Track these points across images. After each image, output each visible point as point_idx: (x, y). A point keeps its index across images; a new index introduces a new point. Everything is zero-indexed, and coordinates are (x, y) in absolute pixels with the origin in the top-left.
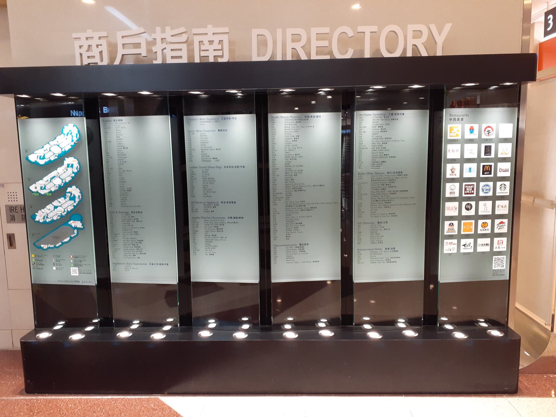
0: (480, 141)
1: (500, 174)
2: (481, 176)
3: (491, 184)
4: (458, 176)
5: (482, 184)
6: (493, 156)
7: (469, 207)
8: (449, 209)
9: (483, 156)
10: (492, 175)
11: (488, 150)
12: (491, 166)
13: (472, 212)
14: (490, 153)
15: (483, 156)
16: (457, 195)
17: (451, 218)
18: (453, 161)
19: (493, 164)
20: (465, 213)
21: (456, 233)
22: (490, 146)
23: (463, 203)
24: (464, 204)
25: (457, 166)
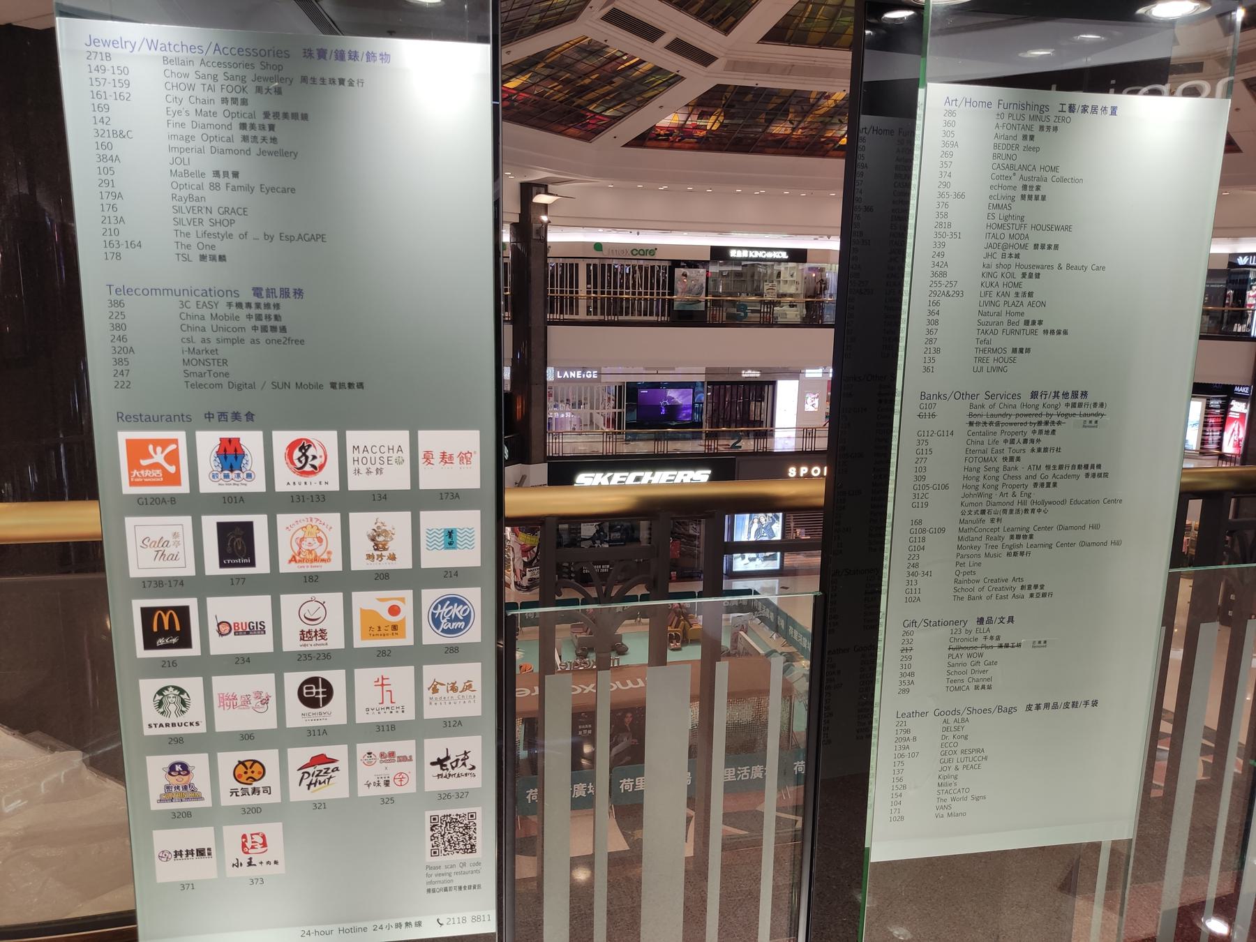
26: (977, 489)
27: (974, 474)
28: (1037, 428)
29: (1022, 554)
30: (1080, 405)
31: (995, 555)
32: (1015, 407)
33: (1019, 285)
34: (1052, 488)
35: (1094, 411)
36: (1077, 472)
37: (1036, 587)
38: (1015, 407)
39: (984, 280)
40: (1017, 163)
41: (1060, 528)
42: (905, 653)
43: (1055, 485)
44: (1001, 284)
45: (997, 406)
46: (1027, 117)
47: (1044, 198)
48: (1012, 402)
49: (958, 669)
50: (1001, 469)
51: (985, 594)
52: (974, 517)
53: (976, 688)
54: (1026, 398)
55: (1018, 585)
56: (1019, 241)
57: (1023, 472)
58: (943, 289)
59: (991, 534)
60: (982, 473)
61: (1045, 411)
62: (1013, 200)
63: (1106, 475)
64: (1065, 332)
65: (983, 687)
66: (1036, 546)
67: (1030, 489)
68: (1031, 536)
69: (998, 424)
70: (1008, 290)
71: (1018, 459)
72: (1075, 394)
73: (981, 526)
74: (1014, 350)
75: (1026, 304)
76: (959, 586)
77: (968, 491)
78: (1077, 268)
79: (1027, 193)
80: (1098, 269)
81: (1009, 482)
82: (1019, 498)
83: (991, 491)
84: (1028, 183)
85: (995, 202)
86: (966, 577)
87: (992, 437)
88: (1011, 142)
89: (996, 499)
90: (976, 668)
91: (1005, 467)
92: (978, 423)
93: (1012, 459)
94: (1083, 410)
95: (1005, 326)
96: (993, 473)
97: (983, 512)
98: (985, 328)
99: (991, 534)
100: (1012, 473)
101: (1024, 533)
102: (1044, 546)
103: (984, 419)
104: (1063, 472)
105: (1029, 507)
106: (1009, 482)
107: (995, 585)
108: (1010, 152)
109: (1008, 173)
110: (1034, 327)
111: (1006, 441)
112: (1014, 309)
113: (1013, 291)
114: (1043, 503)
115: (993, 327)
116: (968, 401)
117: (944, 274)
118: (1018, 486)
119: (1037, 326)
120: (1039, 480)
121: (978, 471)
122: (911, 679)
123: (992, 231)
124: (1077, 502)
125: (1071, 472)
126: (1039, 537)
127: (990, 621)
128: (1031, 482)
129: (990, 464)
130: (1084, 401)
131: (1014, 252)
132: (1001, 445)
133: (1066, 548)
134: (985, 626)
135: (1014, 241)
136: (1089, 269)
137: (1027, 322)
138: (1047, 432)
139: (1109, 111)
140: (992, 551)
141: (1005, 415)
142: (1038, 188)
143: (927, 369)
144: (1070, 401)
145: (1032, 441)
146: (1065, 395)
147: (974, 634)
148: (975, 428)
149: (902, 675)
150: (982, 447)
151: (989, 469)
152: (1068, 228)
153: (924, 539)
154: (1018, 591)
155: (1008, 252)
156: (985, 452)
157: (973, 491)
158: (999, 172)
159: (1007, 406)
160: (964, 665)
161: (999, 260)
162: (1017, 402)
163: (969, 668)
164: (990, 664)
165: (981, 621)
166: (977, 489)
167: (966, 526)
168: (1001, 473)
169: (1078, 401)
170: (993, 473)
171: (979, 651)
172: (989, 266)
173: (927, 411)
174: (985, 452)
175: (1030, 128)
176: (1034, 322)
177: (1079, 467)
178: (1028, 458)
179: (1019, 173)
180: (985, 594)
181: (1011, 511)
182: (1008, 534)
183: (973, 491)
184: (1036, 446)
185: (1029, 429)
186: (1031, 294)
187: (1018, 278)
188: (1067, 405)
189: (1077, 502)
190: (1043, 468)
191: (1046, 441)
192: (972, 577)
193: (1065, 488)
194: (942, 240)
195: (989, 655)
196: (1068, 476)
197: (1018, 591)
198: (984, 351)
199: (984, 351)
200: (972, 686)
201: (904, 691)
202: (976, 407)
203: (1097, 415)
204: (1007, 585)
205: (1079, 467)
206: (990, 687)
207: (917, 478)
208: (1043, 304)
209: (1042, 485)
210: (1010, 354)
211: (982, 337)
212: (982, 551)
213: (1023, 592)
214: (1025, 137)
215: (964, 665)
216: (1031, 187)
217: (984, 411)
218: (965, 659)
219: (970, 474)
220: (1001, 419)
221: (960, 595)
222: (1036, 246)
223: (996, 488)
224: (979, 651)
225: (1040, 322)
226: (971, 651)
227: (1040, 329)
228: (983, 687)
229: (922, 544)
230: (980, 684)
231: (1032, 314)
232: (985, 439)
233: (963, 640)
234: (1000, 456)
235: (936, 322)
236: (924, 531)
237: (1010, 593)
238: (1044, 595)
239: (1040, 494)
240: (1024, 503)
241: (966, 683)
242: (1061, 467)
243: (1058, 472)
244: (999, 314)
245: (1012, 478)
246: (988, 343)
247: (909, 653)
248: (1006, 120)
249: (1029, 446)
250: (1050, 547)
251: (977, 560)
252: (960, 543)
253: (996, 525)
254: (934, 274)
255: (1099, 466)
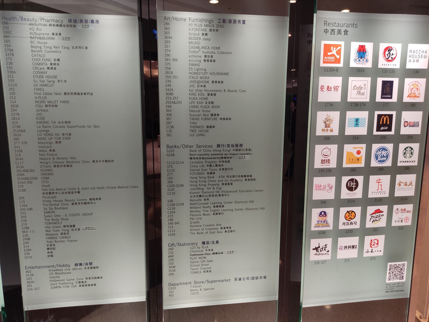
0: (375, 72)
1: (405, 131)
2: (375, 133)
3: (390, 147)
4: (336, 132)
5: (375, 147)
6: (395, 99)
7: (353, 184)
8: (319, 187)
9: (378, 99)
10: (392, 133)
11: (387, 88)
12: (391, 116)
13: (358, 194)
14: (391, 94)
15: (378, 99)
16: (333, 164)
17: (323, 203)
18: (329, 106)
19: (394, 113)
20: (345, 194)
21: (331, 228)
22: (391, 83)
23: (343, 178)
24: (345, 179)
25: (335, 115)
26: (196, 186)
27: (195, 180)
28: (221, 160)
29: (220, 214)
30: (240, 150)
31: (208, 215)
32: (210, 151)
33: (207, 99)
34: (230, 186)
35: (247, 152)
36: (241, 178)
37: (227, 228)
38: (210, 151)
39: (190, 96)
40: (200, 46)
41: (236, 202)
42: (170, 258)
43: (232, 184)
44: (198, 98)
45: (202, 151)
46: (203, 26)
47: (214, 61)
48: (209, 149)
49: (195, 264)
50: (207, 178)
51: (204, 231)
52: (197, 198)
53: (204, 272)
54: (215, 147)
55: (219, 227)
56: (205, 80)
57: (217, 179)
58: (172, 100)
59: (205, 206)
60: (198, 180)
61: (224, 153)
62: (200, 62)
63: (254, 180)
64: (230, 119)
65: (207, 271)
66: (226, 210)
67: (221, 186)
68: (223, 206)
69: (203, 158)
70: (202, 101)
71: (214, 173)
72: (237, 145)
73: (200, 202)
74: (208, 127)
75: (211, 107)
76: (192, 228)
77: (193, 187)
78: (232, 91)
79: (206, 59)
80: (242, 91)
81: (211, 183)
82: (216, 190)
83: (203, 187)
84: (207, 55)
85: (192, 63)
86: (195, 224)
87: (201, 164)
88: (197, 36)
89: (205, 190)
90: (203, 263)
91: (208, 177)
92: (194, 158)
93: (211, 173)
94: (242, 152)
95: (202, 116)
96: (203, 179)
97: (200, 196)
98: (193, 117)
99: (205, 206)
100: (212, 179)
101: (219, 205)
102: (229, 210)
103: (197, 156)
104: (235, 178)
105: (221, 194)
106: (211, 183)
107: (209, 227)
108: (197, 41)
109: (196, 50)
110: (215, 117)
111: (208, 166)
112: (205, 109)
113: (204, 101)
114: (227, 192)
115: (197, 117)
116: (189, 149)
117: (172, 94)
118: (215, 185)
119: (216, 117)
120: (224, 182)
121: (196, 178)
122: (174, 269)
123: (192, 75)
124: (242, 191)
125: (238, 178)
126: (227, 207)
127: (208, 243)
128: (221, 183)
129: (201, 176)
130: (241, 148)
131: (203, 84)
132: (206, 167)
133: (239, 211)
134: (206, 245)
135: (203, 80)
136: (238, 91)
137: (212, 115)
138: (226, 162)
139: (242, 22)
140: (206, 213)
141: (206, 155)
142: (212, 57)
143: (168, 135)
144: (235, 148)
145: (220, 165)
146: (233, 146)
147: (201, 249)
148: (193, 160)
149: (170, 267)
150: (197, 168)
151: (201, 178)
152: (227, 74)
153: (174, 208)
154: (219, 230)
155: (200, 84)
156: (198, 170)
157: (195, 187)
158: (192, 50)
159: (207, 151)
160: (198, 262)
161: (196, 88)
162: (211, 149)
163: (200, 263)
164: (209, 261)
165: (204, 243)
166: (196, 186)
167: (193, 202)
168: (207, 179)
169: (238, 148)
170: (203, 179)
171: (204, 256)
172: (192, 91)
173: (171, 153)
174: (198, 170)
175: (205, 30)
176: (215, 115)
177: (242, 176)
178: (218, 173)
179: (202, 50)
180: (204, 231)
181: (213, 196)
182: (212, 206)
183: (195, 187)
184: (221, 168)
185: (217, 160)
186: (212, 103)
187: (206, 96)
188: (234, 150)
189: (242, 191)
190: (226, 177)
191: (226, 165)
192: (198, 224)
193: (236, 186)
194: (169, 79)
195: (209, 257)
196: (237, 180)
197: (219, 230)
198: (194, 127)
199: (194, 127)
200: (202, 271)
201: (171, 274)
202: (193, 151)
203: (248, 154)
204: (214, 227)
205: (242, 176)
206: (210, 271)
207: (169, 182)
208: (218, 107)
209: (226, 184)
210: (205, 128)
211: (192, 121)
212: (202, 213)
213: (222, 230)
214: (203, 34)
215: (198, 262)
216: (209, 56)
217: (197, 153)
218: (198, 260)
219: (193, 180)
220: (205, 157)
221: (193, 232)
222: (213, 82)
223: (205, 186)
224: (204, 256)
225: (218, 115)
226: (200, 256)
227: (218, 118)
228: (207, 271)
229: (174, 211)
230: (206, 270)
231: (214, 111)
232: (198, 165)
233: (197, 251)
234: (206, 172)
235: (171, 115)
236: (174, 205)
237: (216, 231)
238: (231, 231)
239: (225, 188)
240: (219, 192)
241: (199, 270)
242: (234, 176)
243: (233, 179)
244: (199, 111)
245: (212, 181)
246: (195, 124)
247: (172, 258)
248: (193, 27)
249: (218, 168)
250: (232, 211)
251: (199, 217)
252: (191, 210)
253: (207, 202)
254: (167, 94)
255: (251, 176)
